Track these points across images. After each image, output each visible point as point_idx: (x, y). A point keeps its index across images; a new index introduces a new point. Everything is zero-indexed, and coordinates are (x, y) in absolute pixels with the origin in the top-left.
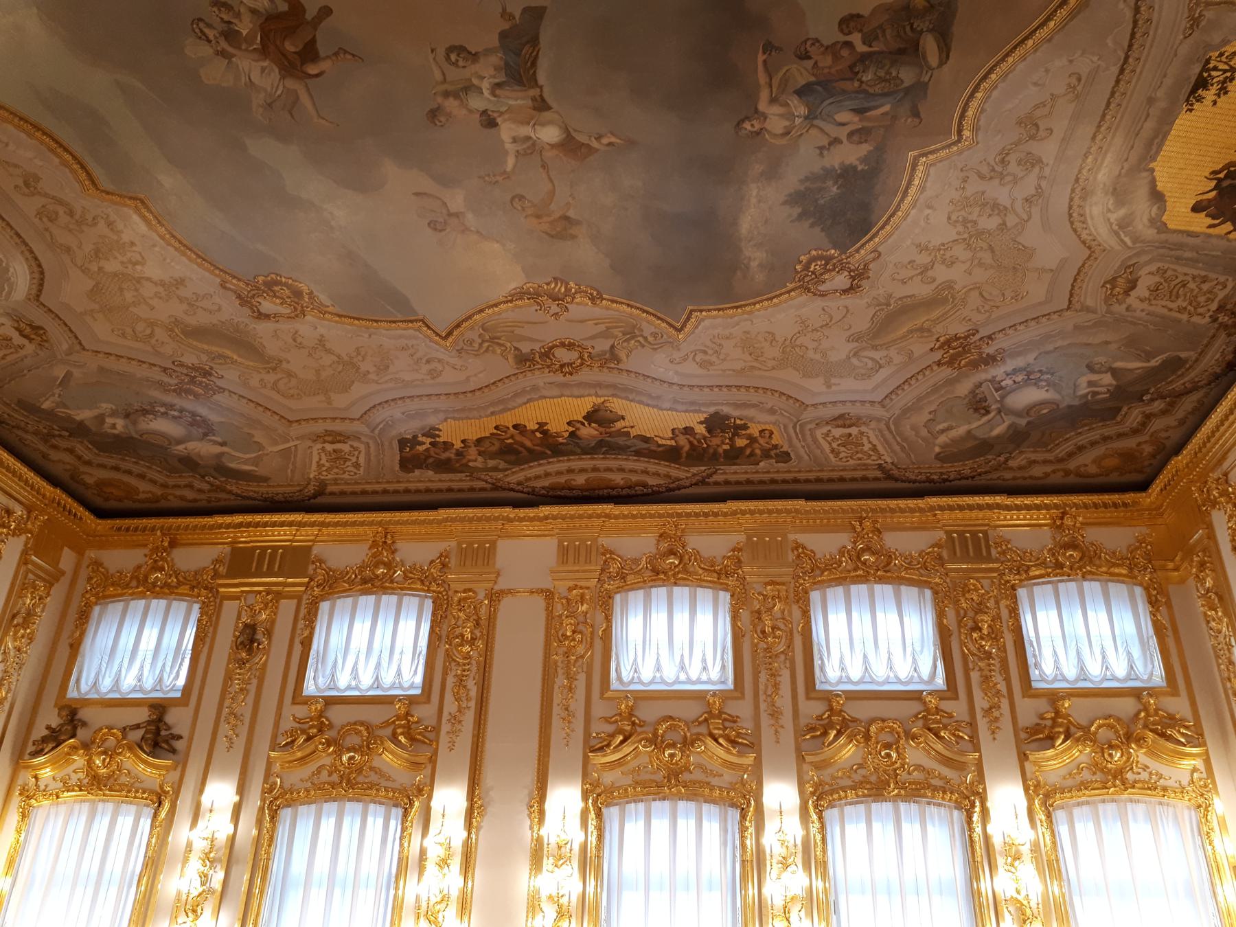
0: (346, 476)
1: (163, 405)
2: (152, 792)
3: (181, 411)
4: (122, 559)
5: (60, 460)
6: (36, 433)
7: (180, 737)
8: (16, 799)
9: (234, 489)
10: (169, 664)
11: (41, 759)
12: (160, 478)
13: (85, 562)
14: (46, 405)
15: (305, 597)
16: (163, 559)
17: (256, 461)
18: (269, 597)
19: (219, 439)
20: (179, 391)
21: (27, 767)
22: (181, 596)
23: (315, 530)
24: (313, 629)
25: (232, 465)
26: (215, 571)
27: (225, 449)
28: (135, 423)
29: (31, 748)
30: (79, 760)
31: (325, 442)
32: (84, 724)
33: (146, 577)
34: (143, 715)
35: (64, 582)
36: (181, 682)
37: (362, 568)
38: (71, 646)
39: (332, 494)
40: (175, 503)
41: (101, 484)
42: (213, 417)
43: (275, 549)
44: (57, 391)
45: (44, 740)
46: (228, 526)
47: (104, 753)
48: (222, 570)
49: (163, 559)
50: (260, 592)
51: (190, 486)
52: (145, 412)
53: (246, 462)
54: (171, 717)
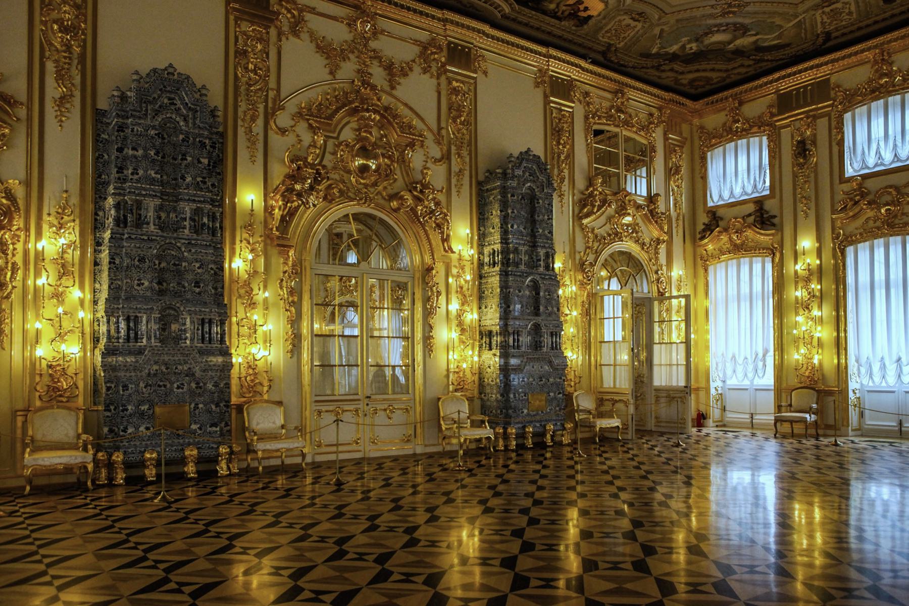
0: (844, 23)
1: (715, 26)
2: (768, 249)
3: (727, 25)
4: (714, 120)
5: (667, 77)
6: (653, 67)
7: (775, 217)
8: (699, 262)
9: (769, 57)
10: (757, 176)
11: (706, 241)
12: (724, 67)
13: (695, 129)
14: (654, 51)
15: (833, 114)
16: (737, 114)
17: (779, 37)
18: (809, 120)
19: (753, 32)
20: (724, 14)
21: (700, 246)
22: (754, 135)
23: (830, 66)
24: (843, 133)
25: (766, 44)
26: (771, 113)
27: (758, 37)
28: (702, 42)
29: (698, 236)
30: (724, 238)
31: (823, 7)
32: (722, 219)
33: (731, 128)
34: (751, 208)
35: (688, 143)
36: (768, 184)
37: (870, 81)
38: (702, 178)
39: (836, 37)
40: (734, 78)
41: (693, 81)
42: (747, 21)
43: (805, 87)
44: (658, 42)
45: (704, 231)
46: (771, 82)
47: (737, 232)
48: (774, 110)
49: (737, 114)
50: (801, 119)
51: (742, 66)
52: (706, 34)
53: (774, 39)
54: (769, 205)
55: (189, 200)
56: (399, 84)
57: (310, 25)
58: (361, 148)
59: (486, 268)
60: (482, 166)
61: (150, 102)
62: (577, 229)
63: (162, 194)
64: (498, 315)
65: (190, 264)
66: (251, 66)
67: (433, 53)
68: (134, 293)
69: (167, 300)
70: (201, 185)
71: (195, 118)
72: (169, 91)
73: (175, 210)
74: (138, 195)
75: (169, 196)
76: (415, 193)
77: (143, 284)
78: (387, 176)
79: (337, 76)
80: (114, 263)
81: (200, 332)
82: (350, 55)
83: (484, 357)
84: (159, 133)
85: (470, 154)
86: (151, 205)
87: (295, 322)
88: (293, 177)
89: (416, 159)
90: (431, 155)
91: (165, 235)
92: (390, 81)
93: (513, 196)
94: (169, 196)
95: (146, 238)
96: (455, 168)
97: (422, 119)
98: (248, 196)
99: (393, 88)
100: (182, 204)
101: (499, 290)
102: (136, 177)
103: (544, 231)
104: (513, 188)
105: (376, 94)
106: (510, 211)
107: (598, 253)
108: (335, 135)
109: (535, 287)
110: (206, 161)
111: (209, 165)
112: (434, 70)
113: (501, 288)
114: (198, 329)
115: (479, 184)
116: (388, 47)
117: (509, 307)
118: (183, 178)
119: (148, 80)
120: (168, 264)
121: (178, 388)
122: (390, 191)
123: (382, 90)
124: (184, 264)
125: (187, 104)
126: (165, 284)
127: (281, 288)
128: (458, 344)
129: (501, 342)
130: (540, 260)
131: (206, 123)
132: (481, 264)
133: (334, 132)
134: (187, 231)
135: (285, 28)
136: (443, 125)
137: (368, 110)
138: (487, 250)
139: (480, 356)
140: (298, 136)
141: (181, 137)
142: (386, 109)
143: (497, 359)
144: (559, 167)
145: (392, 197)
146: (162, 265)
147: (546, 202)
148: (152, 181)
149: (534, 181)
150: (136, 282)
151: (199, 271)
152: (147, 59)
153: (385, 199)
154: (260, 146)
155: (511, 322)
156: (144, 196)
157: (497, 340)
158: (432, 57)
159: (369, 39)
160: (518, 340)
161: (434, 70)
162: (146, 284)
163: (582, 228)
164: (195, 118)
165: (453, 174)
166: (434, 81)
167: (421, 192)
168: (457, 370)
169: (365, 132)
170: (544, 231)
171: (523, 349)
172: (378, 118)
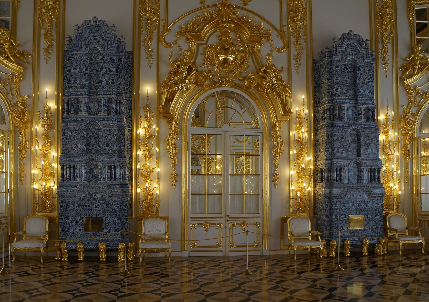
55: (104, 94)
58: (221, 48)
59: (320, 122)
61: (83, 40)
62: (401, 89)
63: (89, 93)
64: (325, 158)
68: (73, 152)
70: (111, 85)
71: (108, 45)
72: (94, 32)
73: (97, 101)
74: (76, 95)
75: (92, 94)
76: (260, 74)
77: (78, 146)
78: (241, 64)
80: (65, 135)
83: (317, 187)
84: (88, 57)
85: (306, 41)
86: (83, 99)
89: (263, 49)
91: (90, 116)
94: (92, 94)
95: (80, 119)
96: (294, 52)
99: (246, 4)
100: (100, 97)
101: (326, 138)
102: (75, 85)
105: (231, 10)
107: (420, 106)
109: (358, 135)
110: (114, 70)
111: (117, 72)
113: (328, 137)
115: (315, 62)
117: (334, 150)
118: (101, 82)
119: (82, 28)
120: (93, 134)
121: (96, 207)
122: (244, 74)
123: (237, 7)
125: (103, 37)
126: (91, 146)
128: (297, 178)
129: (328, 177)
131: (114, 47)
132: (316, 120)
134: (102, 113)
136: (284, 23)
137: (225, 22)
138: (321, 110)
139: (315, 187)
141: (100, 57)
142: (240, 19)
143: (323, 190)
144: (382, 43)
145: (244, 78)
146: (90, 135)
148: (84, 86)
150: (74, 145)
155: (335, 162)
156: (79, 95)
157: (325, 175)
160: (341, 175)
162: (79, 146)
163: (406, 88)
164: (108, 45)
165: (292, 57)
167: (265, 72)
168: (295, 197)
169: (225, 36)
172: (233, 26)
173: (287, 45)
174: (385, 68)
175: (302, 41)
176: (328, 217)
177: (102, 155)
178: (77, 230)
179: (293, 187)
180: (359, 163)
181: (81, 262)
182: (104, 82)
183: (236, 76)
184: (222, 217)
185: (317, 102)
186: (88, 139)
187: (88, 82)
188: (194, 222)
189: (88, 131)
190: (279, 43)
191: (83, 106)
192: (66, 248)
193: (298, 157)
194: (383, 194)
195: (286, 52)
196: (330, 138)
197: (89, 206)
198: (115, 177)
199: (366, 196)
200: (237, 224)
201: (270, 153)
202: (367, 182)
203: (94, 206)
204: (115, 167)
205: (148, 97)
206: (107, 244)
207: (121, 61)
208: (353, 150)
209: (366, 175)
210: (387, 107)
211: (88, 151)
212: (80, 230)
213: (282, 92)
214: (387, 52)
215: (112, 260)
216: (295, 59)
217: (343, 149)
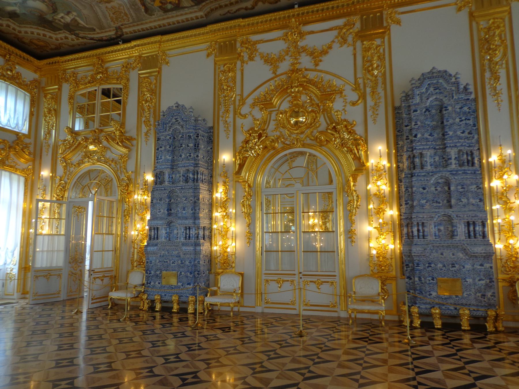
56: (321, 61)
57: (259, 51)
60: (398, 94)
61: (167, 123)
65: (181, 199)
66: (225, 87)
67: (348, 30)
68: (157, 216)
69: (170, 218)
70: (189, 158)
79: (278, 73)
81: (184, 234)
82: (286, 57)
85: (385, 89)
86: (167, 172)
87: (251, 225)
88: (247, 142)
90: (348, 101)
92: (315, 61)
93: (415, 111)
96: (370, 102)
97: (339, 77)
98: (226, 157)
99: (317, 65)
100: (179, 169)
103: (455, 132)
104: (415, 105)
106: (413, 123)
108: (277, 109)
110: (191, 145)
111: (195, 146)
112: (350, 39)
114: (183, 232)
116: (311, 41)
118: (181, 156)
120: (174, 200)
124: (178, 199)
126: (173, 210)
127: (243, 206)
130: (450, 159)
133: (275, 107)
134: (181, 183)
135: (246, 58)
136: (359, 75)
140: (253, 116)
141: (180, 136)
146: (172, 201)
147: (458, 107)
149: (441, 93)
151: (185, 202)
152: (172, 104)
153: (312, 140)
154: (231, 128)
158: (348, 33)
159: (299, 41)
160: (424, 231)
161: (350, 39)
162: (162, 211)
166: (351, 48)
169: (295, 100)
170: (455, 132)
171: (429, 238)
173: (363, 96)
174: (497, 100)
175: (380, 90)
176: (411, 279)
177: (179, 218)
178: (157, 283)
179: (373, 244)
180: (450, 216)
181: (157, 311)
182: (183, 156)
183: (307, 136)
184: (295, 275)
185: (401, 151)
186: (169, 204)
187: (170, 158)
188: (267, 278)
189: (169, 197)
190: (353, 96)
191: (166, 177)
192: (147, 299)
193: (379, 211)
194: (490, 253)
195: (362, 104)
196: (410, 190)
197: (167, 262)
198: (189, 237)
199: (461, 255)
200: (311, 282)
201: (345, 209)
202: (463, 238)
203: (171, 262)
204: (189, 228)
205: (224, 165)
206: (179, 297)
207: (198, 137)
208: (443, 201)
209: (461, 229)
210: (500, 145)
211: (169, 215)
212: (159, 283)
213: (355, 146)
214: (499, 81)
215: (183, 310)
216: (372, 110)
217: (425, 201)
